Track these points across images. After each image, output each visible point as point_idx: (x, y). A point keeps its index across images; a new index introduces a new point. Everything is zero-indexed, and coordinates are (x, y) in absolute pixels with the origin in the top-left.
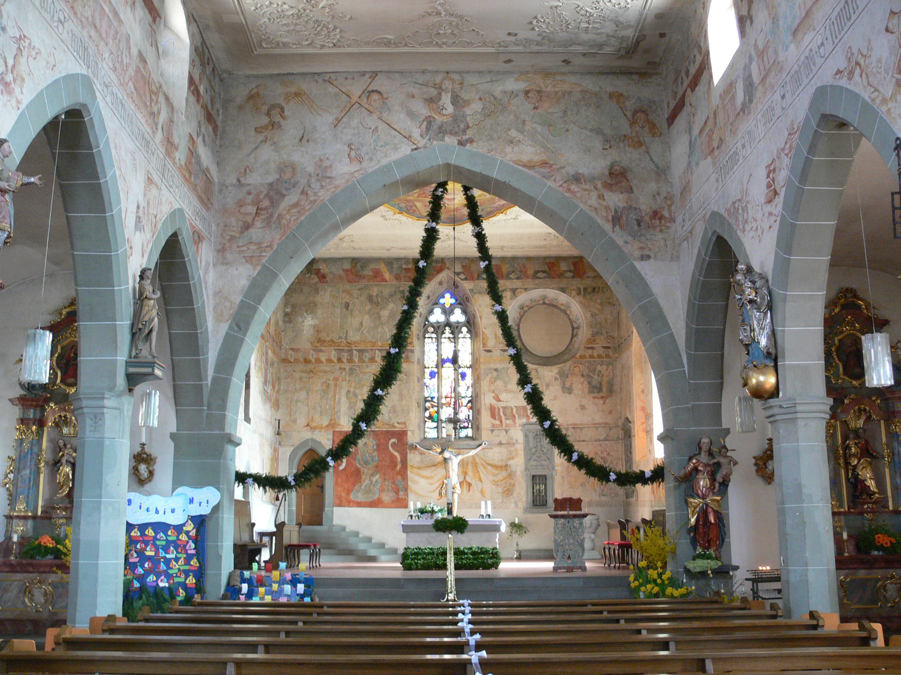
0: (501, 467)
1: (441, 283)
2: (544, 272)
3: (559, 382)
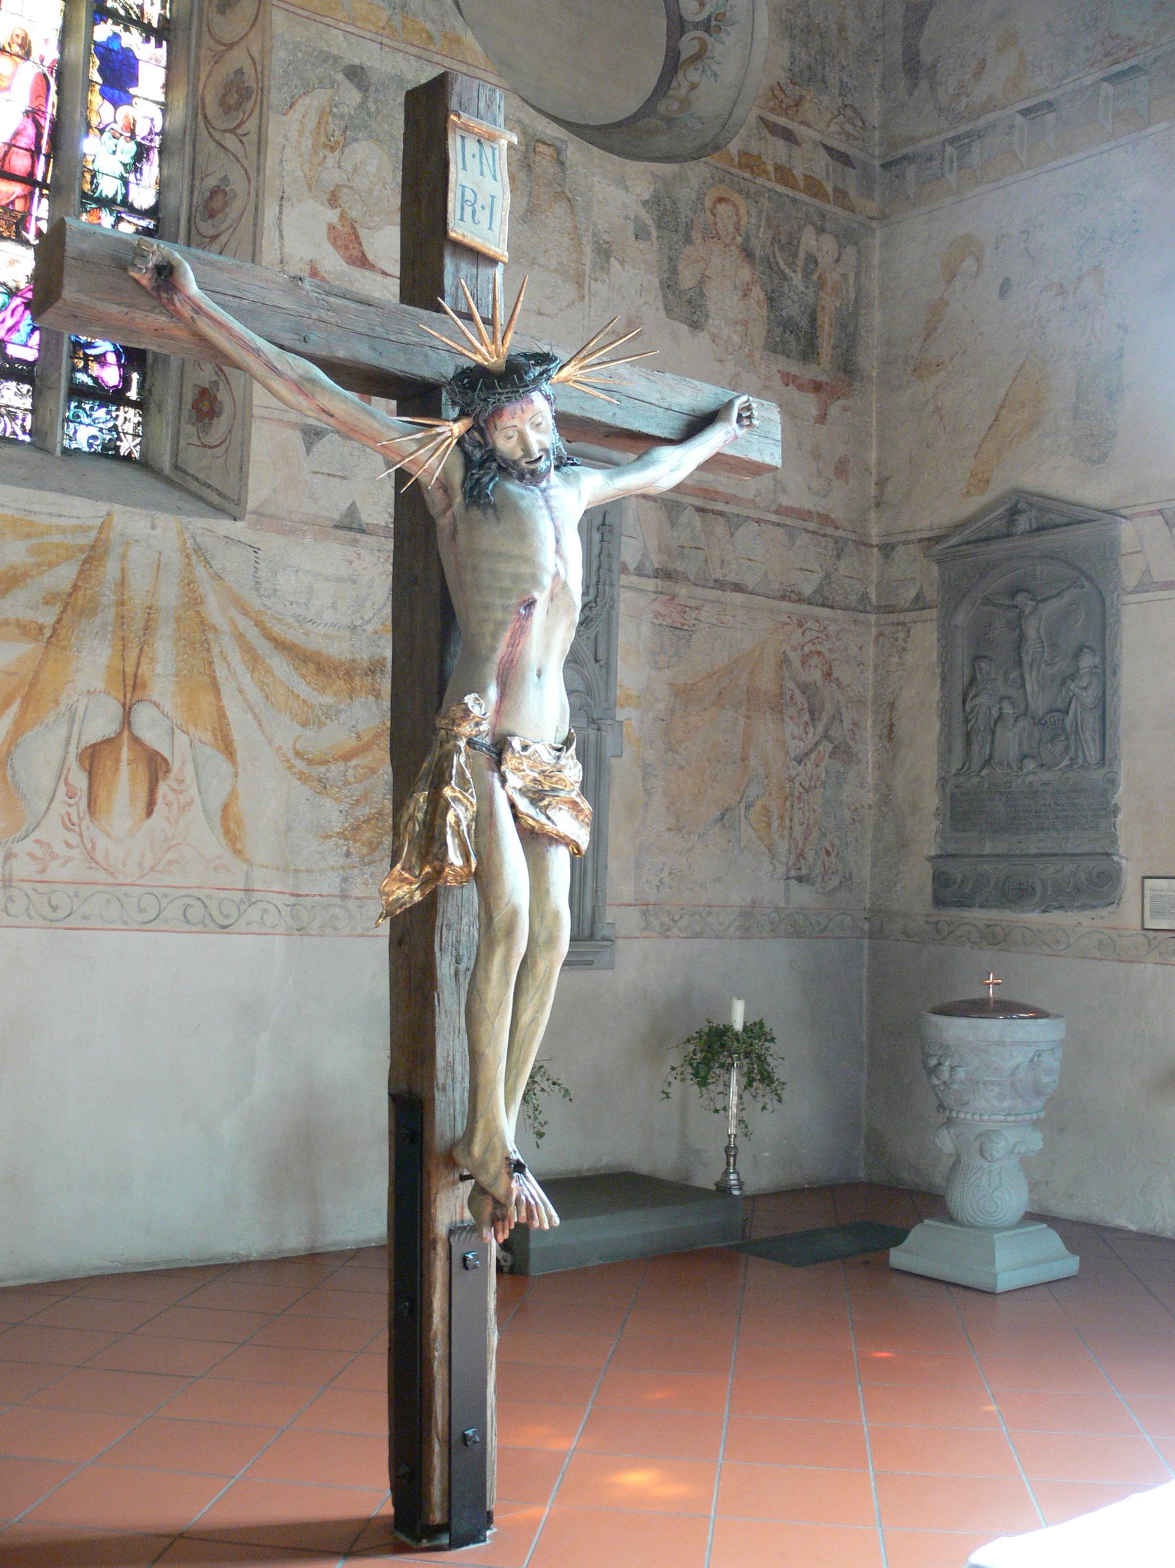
3: (650, 251)
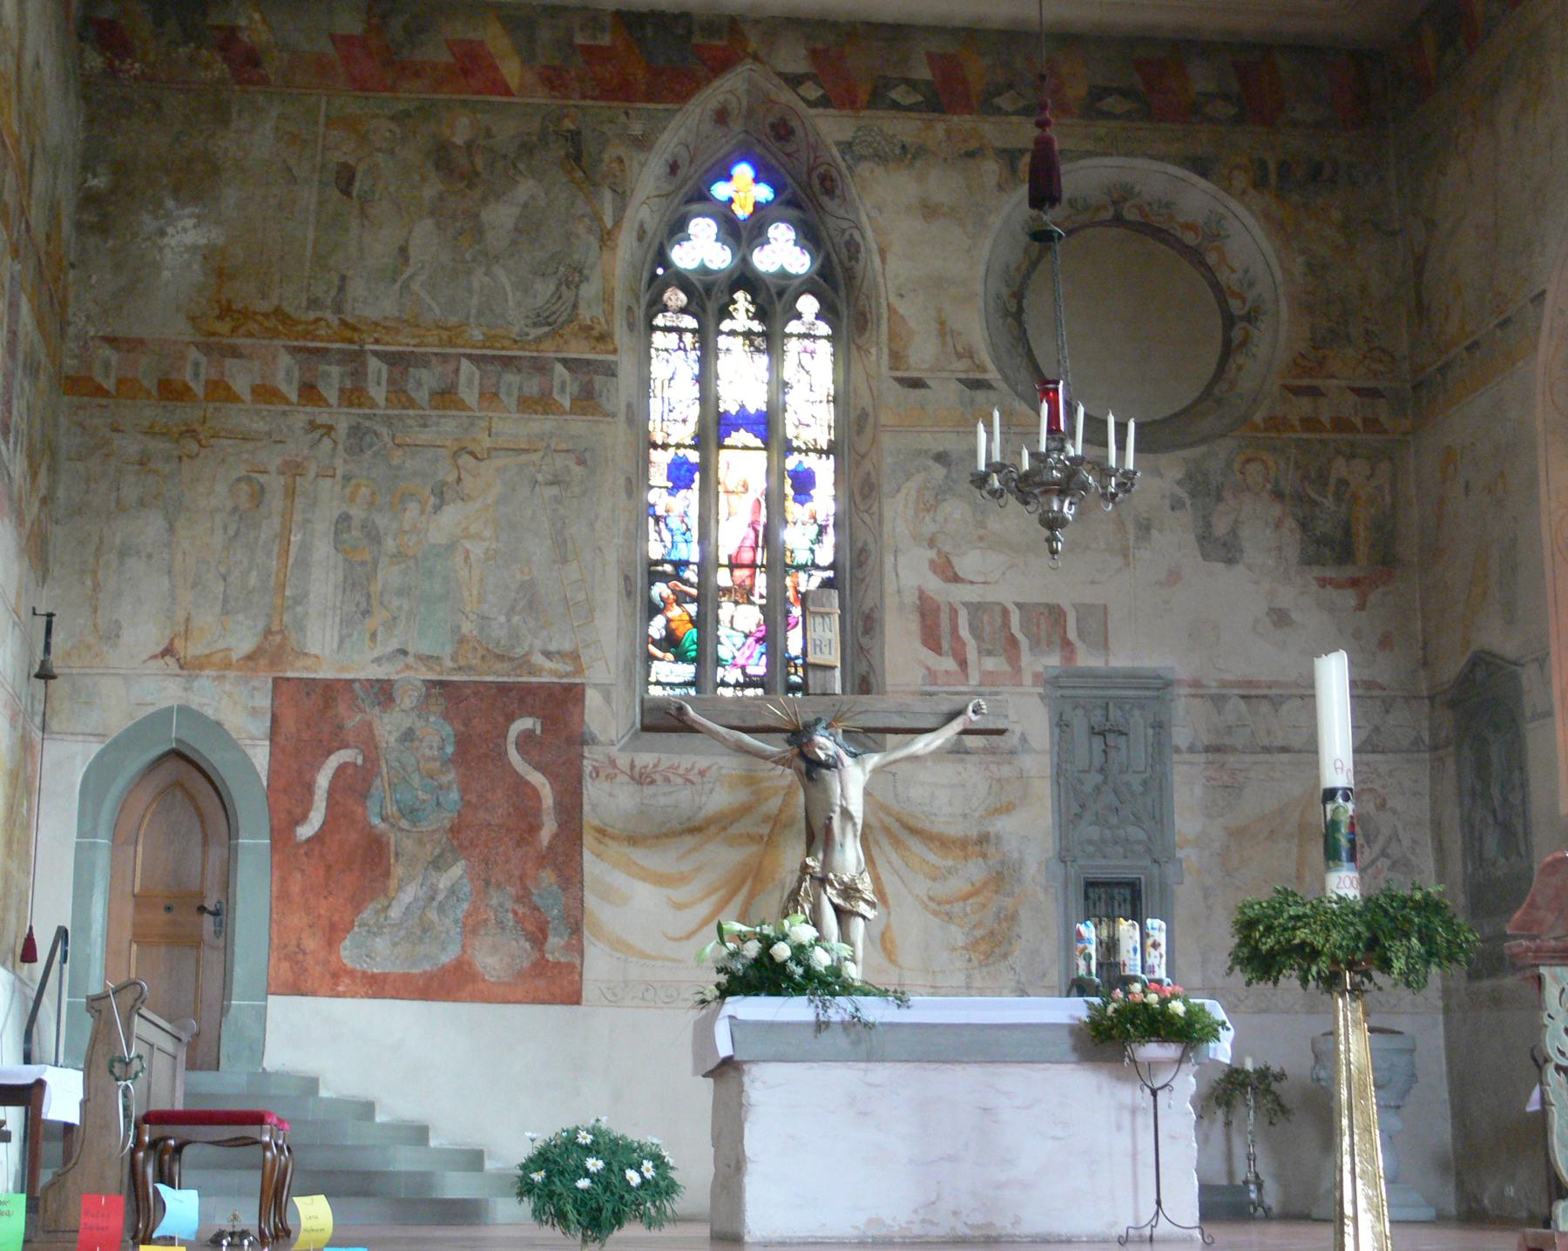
1: (722, 116)
2: (1124, 93)
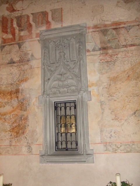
0: (11, 93)
